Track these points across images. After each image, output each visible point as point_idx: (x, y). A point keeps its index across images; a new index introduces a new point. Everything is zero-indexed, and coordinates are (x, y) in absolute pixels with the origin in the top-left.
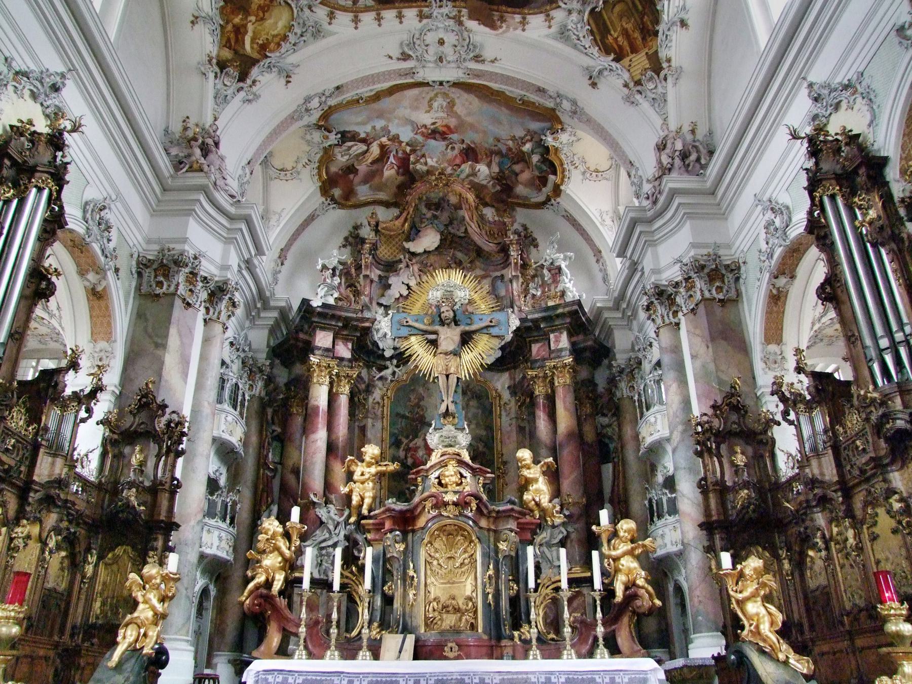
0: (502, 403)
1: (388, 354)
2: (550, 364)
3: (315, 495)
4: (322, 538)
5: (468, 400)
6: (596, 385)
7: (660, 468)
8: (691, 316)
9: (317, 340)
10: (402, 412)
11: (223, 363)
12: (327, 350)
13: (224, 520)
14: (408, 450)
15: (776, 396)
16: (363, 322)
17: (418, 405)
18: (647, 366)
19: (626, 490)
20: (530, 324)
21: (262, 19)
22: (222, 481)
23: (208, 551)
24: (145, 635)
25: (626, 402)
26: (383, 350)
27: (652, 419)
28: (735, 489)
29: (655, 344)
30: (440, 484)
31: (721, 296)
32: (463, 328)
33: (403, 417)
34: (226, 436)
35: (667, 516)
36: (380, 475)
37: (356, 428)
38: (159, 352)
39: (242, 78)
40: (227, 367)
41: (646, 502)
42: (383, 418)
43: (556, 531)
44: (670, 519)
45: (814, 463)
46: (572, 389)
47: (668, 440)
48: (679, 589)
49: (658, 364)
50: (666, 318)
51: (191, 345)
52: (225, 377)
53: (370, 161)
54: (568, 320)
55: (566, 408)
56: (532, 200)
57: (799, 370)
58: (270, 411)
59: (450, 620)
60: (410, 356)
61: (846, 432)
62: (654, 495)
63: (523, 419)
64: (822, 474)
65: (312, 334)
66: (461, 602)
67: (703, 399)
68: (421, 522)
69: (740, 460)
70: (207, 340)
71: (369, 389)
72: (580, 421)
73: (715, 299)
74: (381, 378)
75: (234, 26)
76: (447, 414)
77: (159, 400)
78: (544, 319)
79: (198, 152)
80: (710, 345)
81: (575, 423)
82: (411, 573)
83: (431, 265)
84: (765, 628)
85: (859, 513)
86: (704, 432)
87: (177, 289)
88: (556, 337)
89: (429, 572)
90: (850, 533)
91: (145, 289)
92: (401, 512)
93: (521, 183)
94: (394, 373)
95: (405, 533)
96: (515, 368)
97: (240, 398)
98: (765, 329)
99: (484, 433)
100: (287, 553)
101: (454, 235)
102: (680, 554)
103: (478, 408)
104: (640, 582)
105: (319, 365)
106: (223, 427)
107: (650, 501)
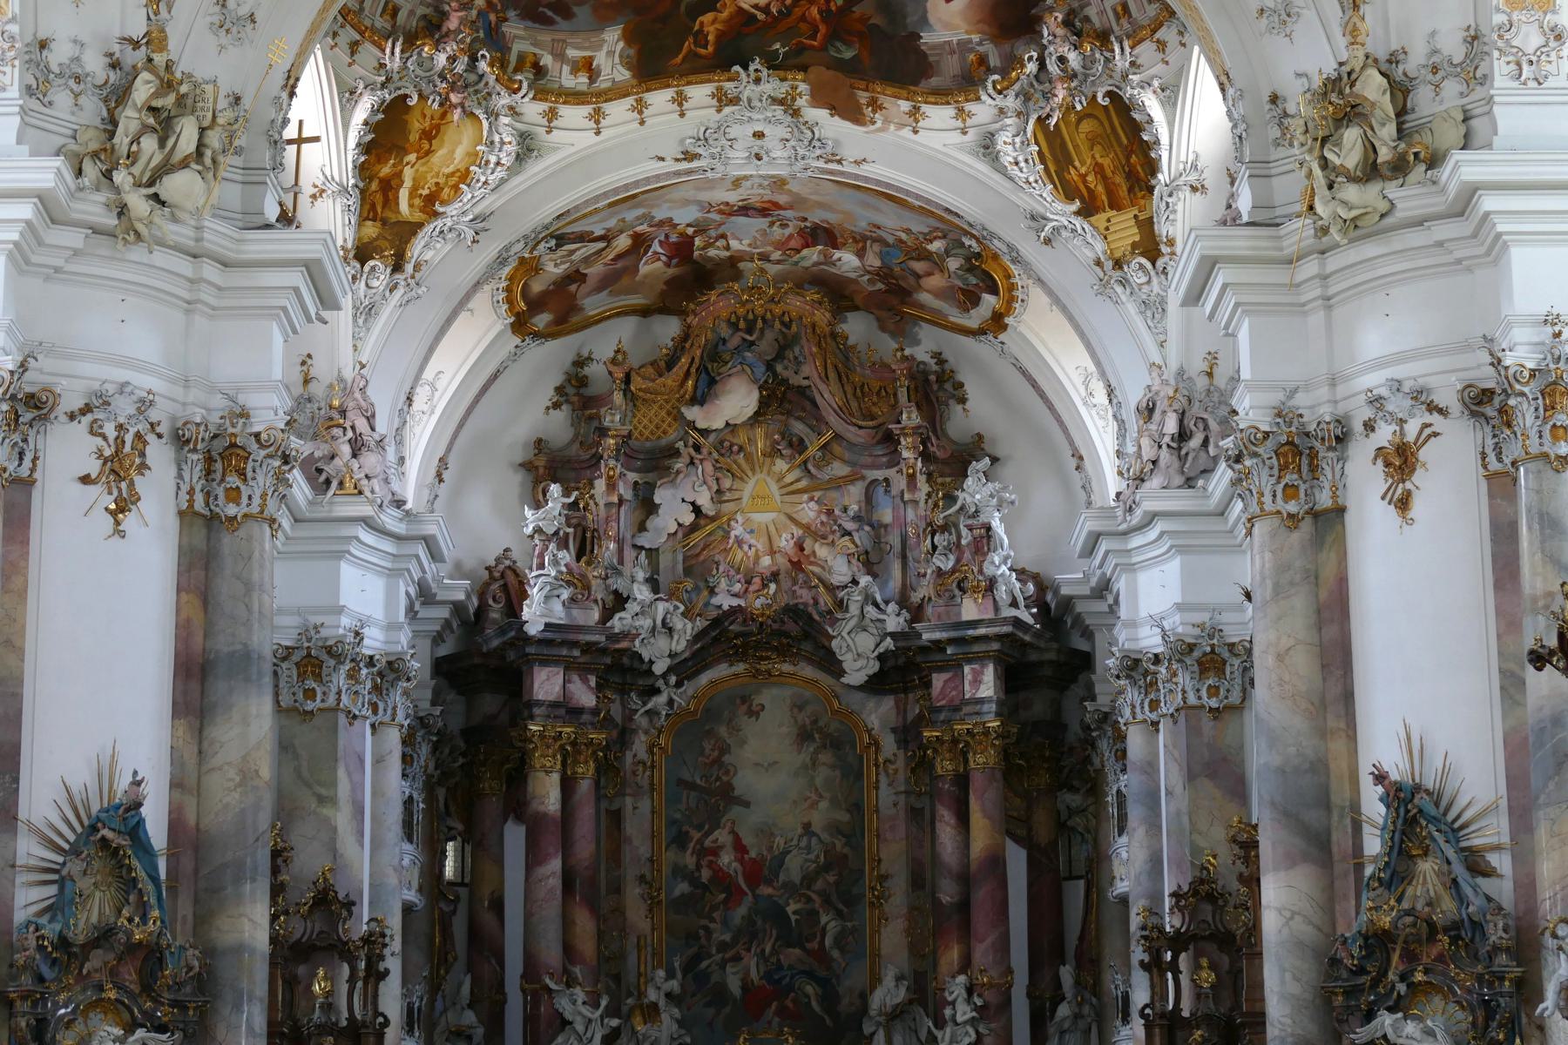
0: (881, 760)
3: (552, 975)
5: (816, 752)
6: (1064, 727)
9: (536, 686)
10: (687, 776)
12: (554, 705)
14: (702, 852)
16: (618, 641)
17: (718, 762)
21: (429, 152)
26: (651, 662)
31: (1214, 703)
33: (692, 786)
38: (326, 811)
39: (397, 268)
42: (652, 790)
43: (960, 1031)
46: (999, 775)
50: (1138, 710)
53: (610, 257)
54: (995, 646)
56: (952, 319)
63: (920, 794)
73: (1203, 706)
74: (647, 712)
75: (381, 181)
77: (341, 896)
78: (951, 641)
79: (346, 450)
83: (741, 449)
87: (339, 700)
91: (286, 700)
93: (928, 291)
94: (671, 702)
96: (906, 691)
99: (843, 817)
101: (785, 381)
103: (833, 767)
105: (542, 736)
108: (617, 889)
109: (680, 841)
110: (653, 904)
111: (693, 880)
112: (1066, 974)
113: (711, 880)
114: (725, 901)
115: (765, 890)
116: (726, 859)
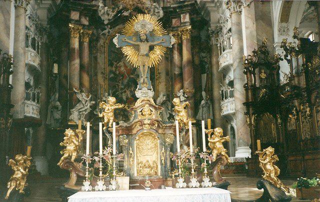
1: (106, 22)
2: (180, 29)
3: (76, 89)
4: (79, 108)
7: (227, 77)
8: (247, 8)
11: (27, 28)
13: (34, 100)
14: (116, 67)
15: (283, 48)
18: (225, 31)
19: (212, 85)
20: (172, 9)
22: (32, 83)
23: (28, 115)
24: (20, 184)
25: (214, 47)
26: (104, 21)
27: (225, 55)
28: (260, 89)
29: (229, 20)
30: (142, 114)
32: (150, 43)
34: (32, 63)
35: (229, 98)
36: (115, 110)
37: (93, 58)
40: (29, 30)
41: (221, 92)
44: (231, 99)
45: (296, 79)
47: (232, 65)
48: (232, 128)
49: (230, 30)
50: (235, 9)
51: (9, 20)
52: (28, 35)
55: (187, 50)
57: (295, 37)
58: (51, 50)
59: (147, 170)
60: (127, 56)
61: (312, 66)
62: (224, 89)
63: (168, 54)
64: (299, 83)
65: (69, 12)
66: (151, 163)
67: (249, 48)
68: (134, 131)
69: (263, 76)
70: (17, 17)
71: (97, 40)
72: (193, 55)
76: (144, 83)
78: (179, 7)
80: (255, 23)
81: (191, 57)
82: (131, 152)
84: (273, 175)
85: (313, 101)
86: (248, 64)
88: (184, 16)
89: (138, 151)
90: (308, 109)
92: (126, 127)
94: (109, 32)
95: (128, 135)
97: (36, 45)
98: (282, 15)
100: (77, 143)
102: (234, 114)
104: (223, 153)
106: (30, 59)
107: (222, 91)
108: (96, 75)
109: (111, 65)
110: (105, 78)
111: (115, 74)
112: (204, 93)
113: (119, 73)
114: (122, 79)
115: (132, 76)
116: (122, 69)
